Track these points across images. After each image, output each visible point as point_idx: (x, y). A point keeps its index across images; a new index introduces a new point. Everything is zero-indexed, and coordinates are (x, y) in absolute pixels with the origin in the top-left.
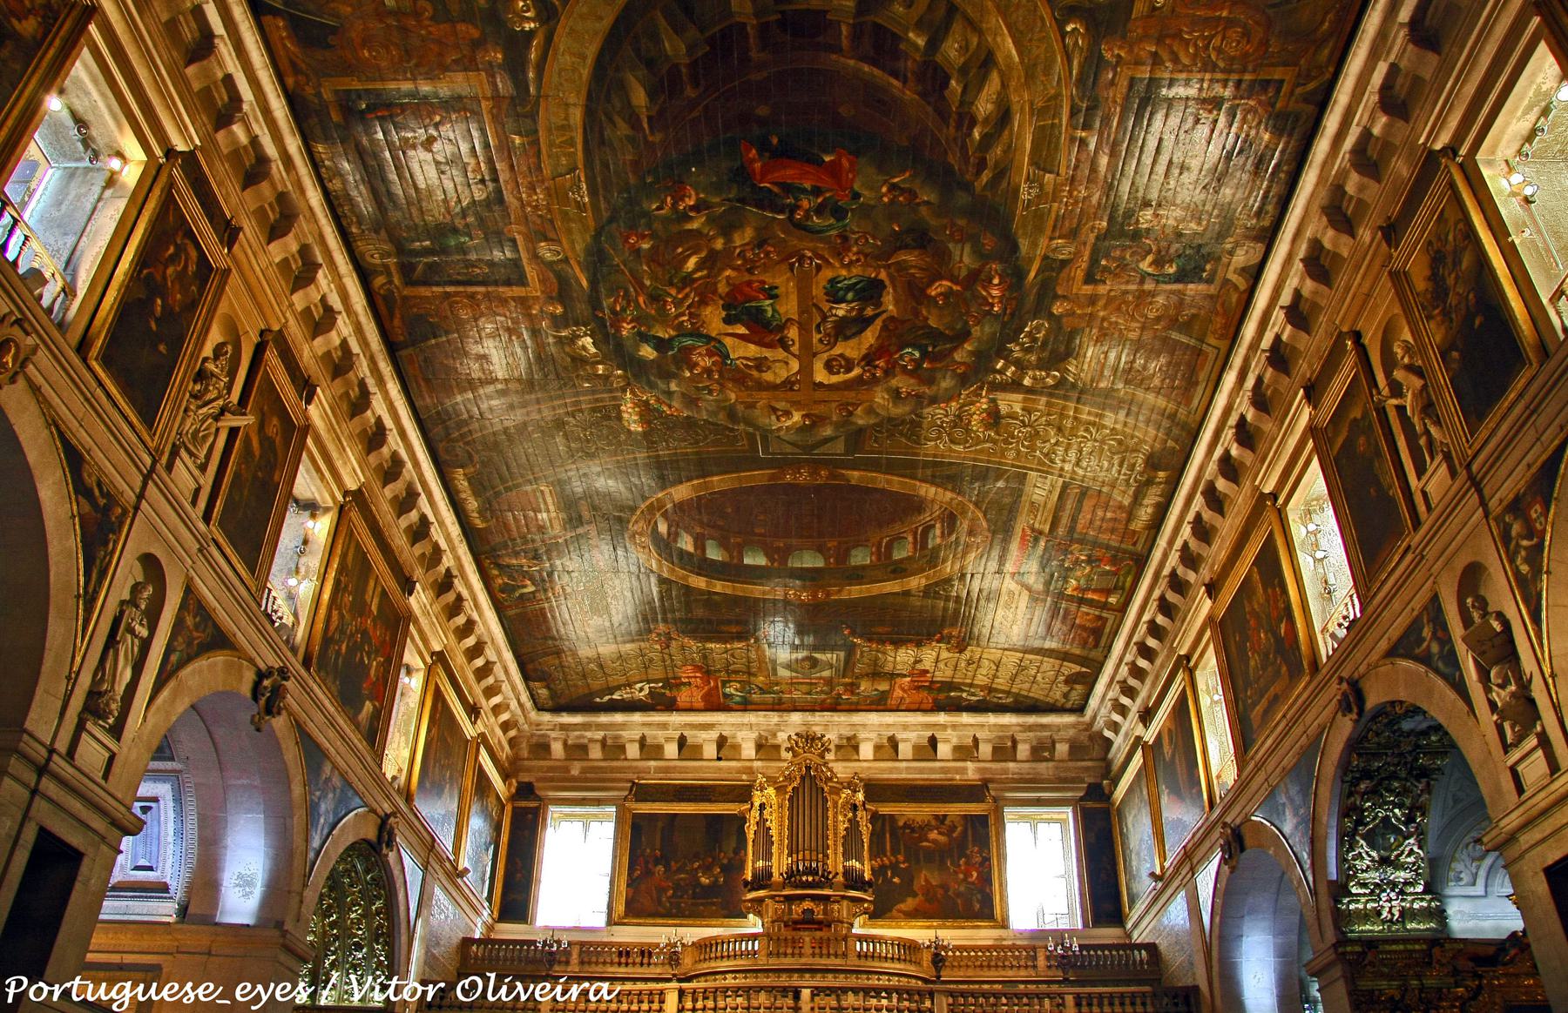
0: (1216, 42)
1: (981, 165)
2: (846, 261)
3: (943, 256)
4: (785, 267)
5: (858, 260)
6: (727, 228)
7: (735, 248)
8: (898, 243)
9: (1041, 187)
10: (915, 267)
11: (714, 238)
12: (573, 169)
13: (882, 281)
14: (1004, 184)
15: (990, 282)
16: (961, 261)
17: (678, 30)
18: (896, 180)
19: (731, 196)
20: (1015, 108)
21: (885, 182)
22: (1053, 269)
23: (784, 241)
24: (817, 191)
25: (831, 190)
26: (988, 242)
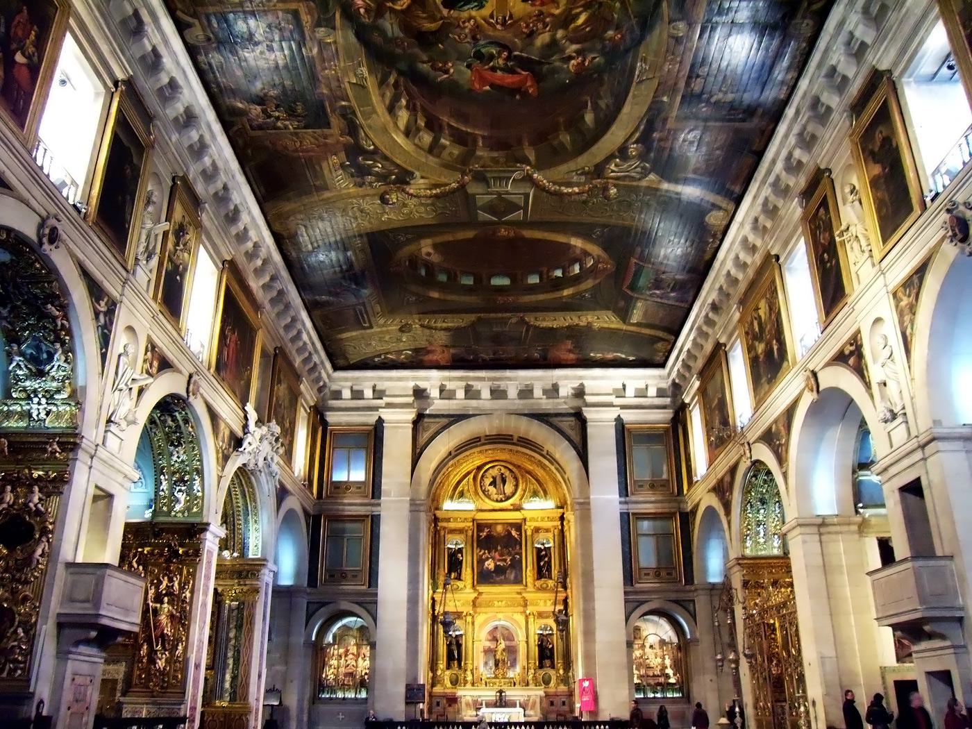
0: (298, 144)
1: (396, 85)
2: (472, 22)
3: (406, 27)
4: (516, 16)
5: (464, 22)
6: (553, 45)
7: (549, 31)
8: (441, 34)
9: (356, 75)
10: (424, 18)
11: (563, 38)
12: (641, 82)
13: (445, 7)
14: (379, 76)
15: (366, 9)
16: (392, 24)
17: (562, 144)
18: (445, 76)
19: (547, 66)
20: (387, 114)
21: (451, 75)
22: (326, 20)
23: (516, 36)
24: (493, 69)
25: (486, 70)
26: (377, 38)
